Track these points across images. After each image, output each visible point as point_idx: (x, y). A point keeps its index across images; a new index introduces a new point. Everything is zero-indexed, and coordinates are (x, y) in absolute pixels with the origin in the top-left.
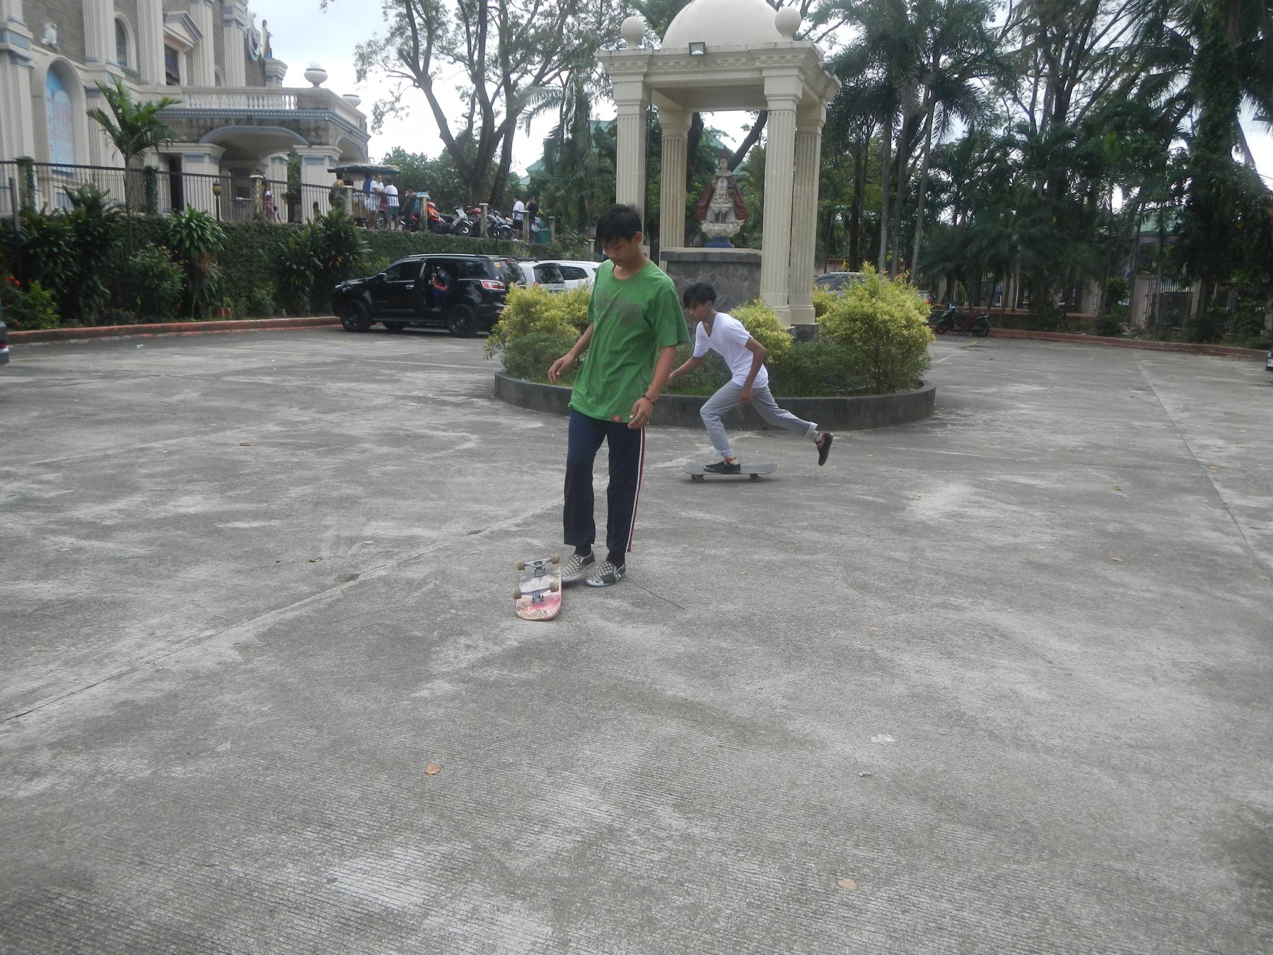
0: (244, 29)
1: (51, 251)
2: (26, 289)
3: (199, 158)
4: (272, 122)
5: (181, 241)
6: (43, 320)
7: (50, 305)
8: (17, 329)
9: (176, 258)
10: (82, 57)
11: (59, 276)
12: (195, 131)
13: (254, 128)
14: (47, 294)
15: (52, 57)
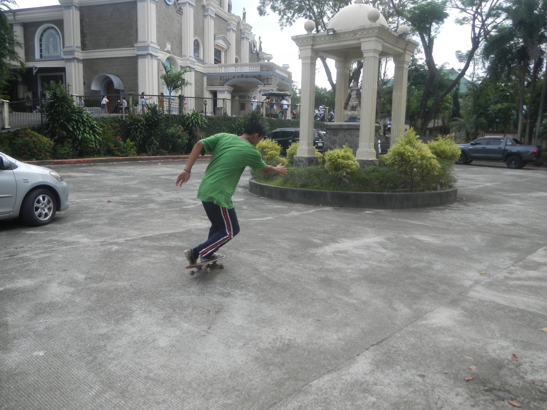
0: (249, 41)
1: (135, 127)
2: (125, 142)
3: (223, 92)
4: (250, 77)
5: (189, 124)
6: (130, 153)
7: (132, 148)
8: (120, 156)
9: (185, 130)
10: (181, 55)
11: (138, 137)
12: (222, 81)
13: (244, 79)
14: (131, 143)
15: (169, 55)
